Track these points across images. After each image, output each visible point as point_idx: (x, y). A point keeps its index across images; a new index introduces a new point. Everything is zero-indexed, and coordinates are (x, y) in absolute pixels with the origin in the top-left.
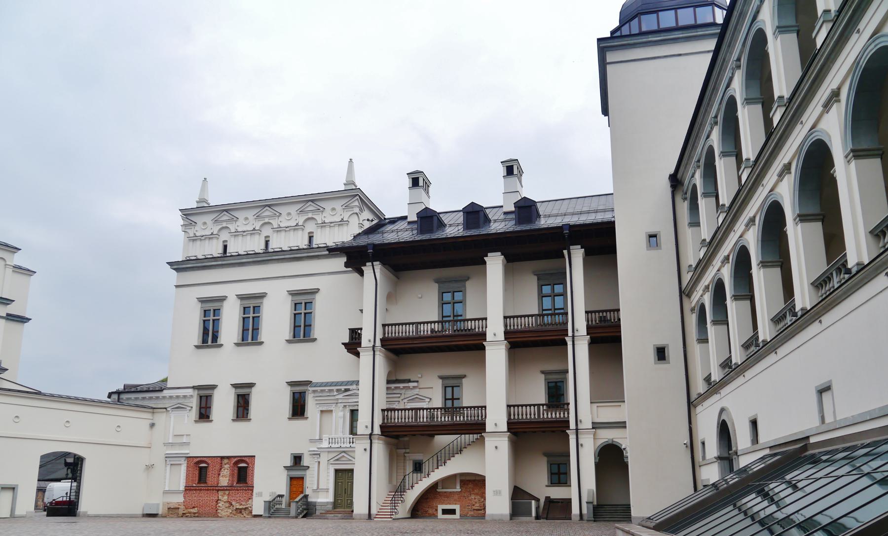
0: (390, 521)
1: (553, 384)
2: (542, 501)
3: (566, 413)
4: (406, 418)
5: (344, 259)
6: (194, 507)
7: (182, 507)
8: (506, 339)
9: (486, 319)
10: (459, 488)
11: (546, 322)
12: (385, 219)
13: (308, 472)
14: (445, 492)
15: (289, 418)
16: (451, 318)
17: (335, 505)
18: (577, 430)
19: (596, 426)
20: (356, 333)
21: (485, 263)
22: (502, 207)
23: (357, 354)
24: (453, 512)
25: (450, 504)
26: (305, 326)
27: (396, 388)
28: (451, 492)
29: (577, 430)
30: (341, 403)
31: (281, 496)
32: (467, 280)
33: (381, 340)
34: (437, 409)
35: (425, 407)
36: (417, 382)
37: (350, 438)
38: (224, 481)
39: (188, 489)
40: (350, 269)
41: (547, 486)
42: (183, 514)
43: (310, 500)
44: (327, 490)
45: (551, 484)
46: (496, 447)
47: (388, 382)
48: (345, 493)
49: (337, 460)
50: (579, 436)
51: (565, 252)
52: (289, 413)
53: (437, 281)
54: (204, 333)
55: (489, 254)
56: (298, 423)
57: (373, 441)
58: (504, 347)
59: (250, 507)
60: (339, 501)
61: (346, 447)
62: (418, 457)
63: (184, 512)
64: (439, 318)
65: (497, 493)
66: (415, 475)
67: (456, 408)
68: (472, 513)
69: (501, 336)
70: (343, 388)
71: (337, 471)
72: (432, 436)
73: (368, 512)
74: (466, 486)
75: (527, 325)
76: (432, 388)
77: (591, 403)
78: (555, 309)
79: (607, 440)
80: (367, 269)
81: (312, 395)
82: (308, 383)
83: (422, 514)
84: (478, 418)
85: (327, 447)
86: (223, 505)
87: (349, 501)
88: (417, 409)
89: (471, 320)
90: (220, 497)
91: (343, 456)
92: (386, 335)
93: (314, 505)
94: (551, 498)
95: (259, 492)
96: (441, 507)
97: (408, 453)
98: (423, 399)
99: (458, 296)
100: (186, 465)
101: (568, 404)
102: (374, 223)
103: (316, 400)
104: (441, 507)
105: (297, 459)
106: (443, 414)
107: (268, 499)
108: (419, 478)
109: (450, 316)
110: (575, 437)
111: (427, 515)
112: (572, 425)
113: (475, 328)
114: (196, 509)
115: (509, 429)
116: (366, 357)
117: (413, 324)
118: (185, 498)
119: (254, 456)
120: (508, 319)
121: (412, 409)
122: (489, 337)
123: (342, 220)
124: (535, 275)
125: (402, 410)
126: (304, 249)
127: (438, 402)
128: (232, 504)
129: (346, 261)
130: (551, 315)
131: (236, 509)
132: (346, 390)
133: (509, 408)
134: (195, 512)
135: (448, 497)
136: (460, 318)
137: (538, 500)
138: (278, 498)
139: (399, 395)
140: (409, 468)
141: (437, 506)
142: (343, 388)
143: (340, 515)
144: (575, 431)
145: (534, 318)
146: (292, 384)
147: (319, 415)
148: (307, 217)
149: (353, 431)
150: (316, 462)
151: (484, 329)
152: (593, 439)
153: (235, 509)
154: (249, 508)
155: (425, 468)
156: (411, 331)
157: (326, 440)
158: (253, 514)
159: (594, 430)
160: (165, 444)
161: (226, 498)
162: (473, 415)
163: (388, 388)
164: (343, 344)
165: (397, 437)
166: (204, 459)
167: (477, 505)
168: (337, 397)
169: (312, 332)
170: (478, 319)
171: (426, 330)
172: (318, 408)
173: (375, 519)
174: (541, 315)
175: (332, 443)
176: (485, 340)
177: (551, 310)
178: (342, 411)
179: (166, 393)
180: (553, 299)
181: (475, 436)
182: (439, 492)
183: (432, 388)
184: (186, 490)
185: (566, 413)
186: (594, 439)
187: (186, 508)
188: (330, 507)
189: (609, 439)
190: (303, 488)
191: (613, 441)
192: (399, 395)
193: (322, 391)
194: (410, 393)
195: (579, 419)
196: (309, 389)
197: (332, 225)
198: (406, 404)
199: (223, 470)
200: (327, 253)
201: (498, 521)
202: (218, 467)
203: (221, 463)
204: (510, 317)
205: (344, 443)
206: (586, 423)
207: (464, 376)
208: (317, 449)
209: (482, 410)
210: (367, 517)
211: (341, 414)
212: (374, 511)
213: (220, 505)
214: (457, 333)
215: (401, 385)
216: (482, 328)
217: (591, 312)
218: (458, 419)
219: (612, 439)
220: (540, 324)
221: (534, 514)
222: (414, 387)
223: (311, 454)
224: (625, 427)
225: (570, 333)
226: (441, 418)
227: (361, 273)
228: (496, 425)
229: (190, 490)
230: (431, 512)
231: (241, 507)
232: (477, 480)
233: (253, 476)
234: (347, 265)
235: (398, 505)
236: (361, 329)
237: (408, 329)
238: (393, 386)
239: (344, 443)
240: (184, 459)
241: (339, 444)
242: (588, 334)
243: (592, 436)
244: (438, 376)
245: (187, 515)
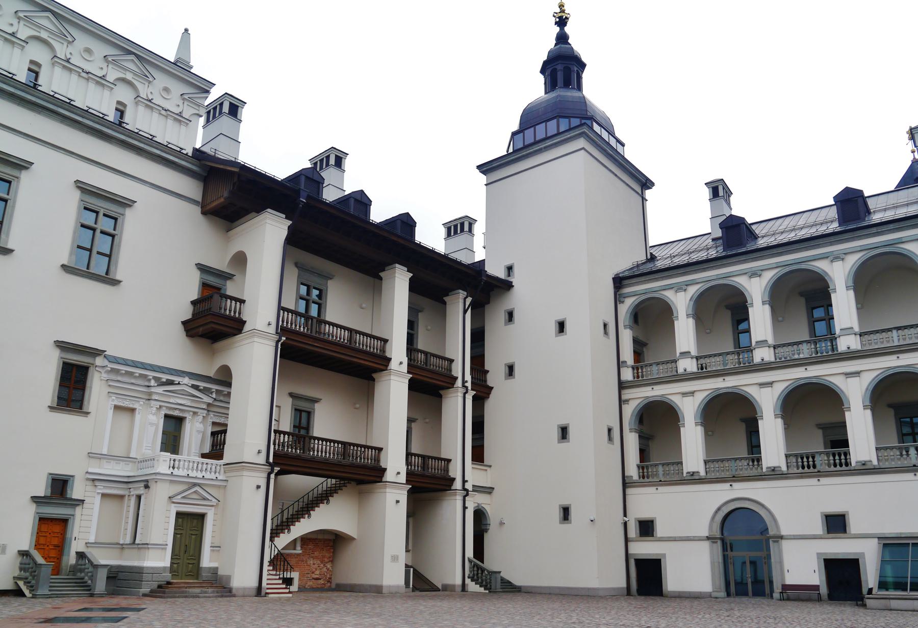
0: (288, 599)
10: (299, 548)
15: (50, 407)
44: (163, 547)
49: (205, 499)
61: (196, 478)
68: (311, 583)
74: (305, 546)
82: (95, 353)
103: (109, 385)
132: (170, 383)
142: (165, 377)
146: (62, 346)
148: (123, 76)
150: (98, 493)
157: (166, 461)
160: (91, 455)
167: (317, 572)
168: (153, 390)
193: (128, 374)
210: (254, 592)
221: (411, 586)
223: (88, 479)
232: (320, 539)
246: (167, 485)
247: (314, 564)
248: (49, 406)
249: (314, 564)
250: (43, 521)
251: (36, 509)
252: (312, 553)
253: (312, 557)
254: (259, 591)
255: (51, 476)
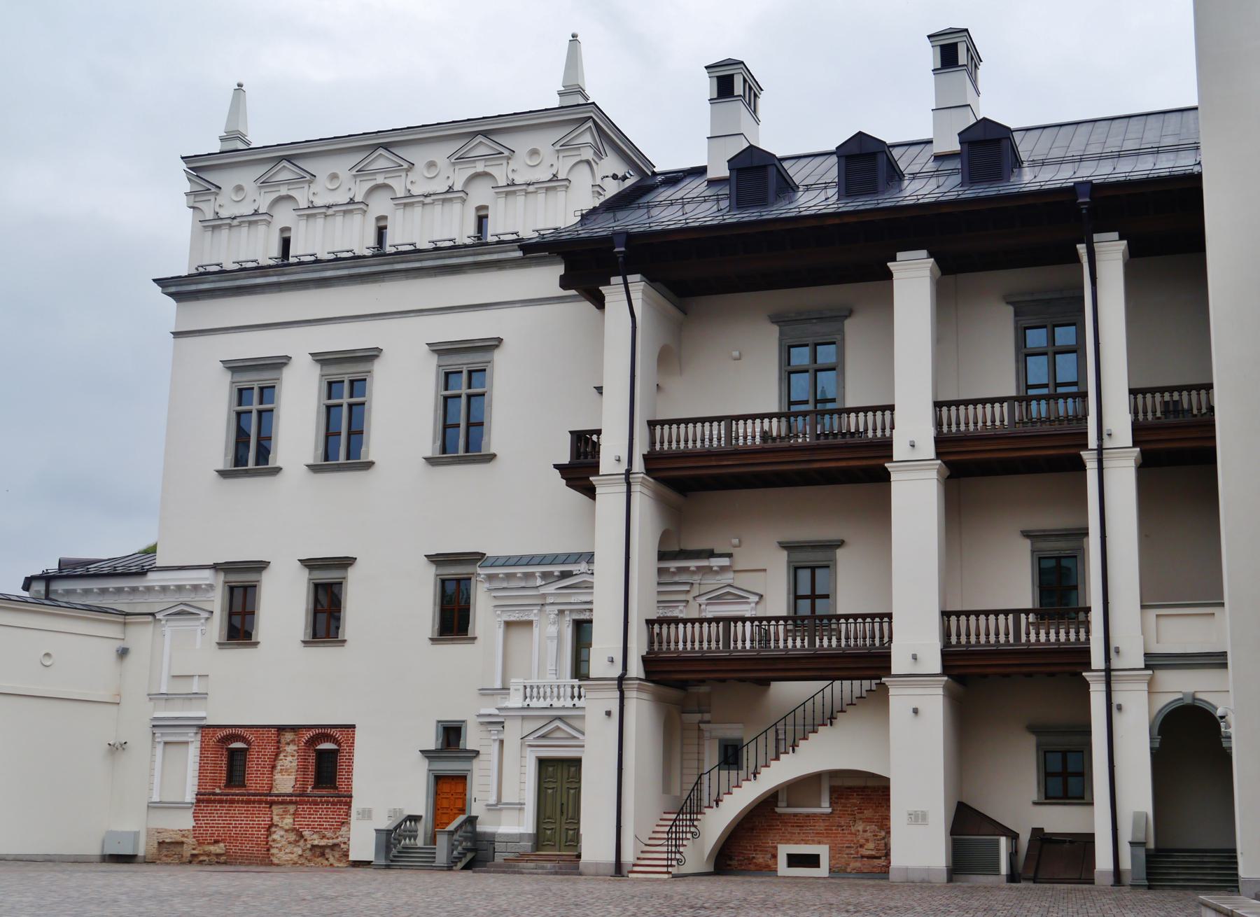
0: (665, 880)
1: (1052, 563)
2: (1025, 838)
3: (1082, 631)
4: (705, 641)
5: (560, 270)
6: (216, 842)
7: (191, 840)
8: (939, 455)
9: (891, 408)
10: (828, 805)
11: (1034, 415)
12: (654, 174)
13: (476, 765)
14: (795, 815)
15: (432, 639)
16: (810, 407)
17: (539, 840)
18: (1108, 671)
19: (1155, 662)
20: (587, 440)
21: (889, 276)
22: (930, 142)
23: (590, 492)
24: (813, 861)
25: (806, 842)
26: (469, 425)
27: (681, 570)
28: (808, 815)
29: (1108, 671)
30: (552, 604)
31: (415, 819)
32: (846, 317)
33: (646, 458)
34: (777, 619)
35: (748, 615)
36: (730, 555)
37: (573, 687)
38: (285, 783)
39: (203, 799)
40: (573, 292)
41: (1035, 803)
42: (193, 856)
43: (481, 828)
44: (520, 806)
45: (1046, 798)
46: (916, 711)
47: (662, 556)
48: (562, 812)
49: (543, 737)
50: (1114, 686)
51: (1082, 248)
52: (433, 626)
53: (777, 319)
54: (237, 443)
55: (900, 255)
56: (454, 651)
57: (627, 694)
58: (934, 474)
59: (345, 843)
60: (549, 832)
61: (564, 708)
62: (732, 731)
63: (194, 852)
64: (780, 407)
65: (918, 818)
66: (724, 773)
67: (821, 618)
68: (858, 864)
69: (927, 448)
70: (557, 569)
71: (542, 763)
72: (766, 683)
73: (614, 859)
74: (843, 801)
75: (989, 423)
76: (765, 570)
77: (1143, 607)
78: (1057, 385)
79: (1180, 696)
80: (613, 293)
81: (487, 585)
82: (476, 558)
83: (741, 865)
84: (873, 641)
85: (520, 705)
86: (282, 837)
87: (571, 832)
88: (728, 621)
89: (857, 410)
90: (276, 818)
91: (558, 728)
92: (658, 447)
93: (490, 839)
94: (1046, 831)
95: (364, 810)
96: (784, 850)
97: (709, 722)
98: (743, 597)
99: (826, 354)
100: (198, 744)
101: (1088, 610)
102: (629, 183)
103: (494, 597)
104: (784, 850)
105: (451, 734)
106: (790, 631)
107: (386, 824)
108: (733, 782)
109: (806, 402)
110: (1103, 687)
111: (752, 866)
112: (1097, 660)
113: (866, 430)
114: (222, 845)
115: (947, 669)
116: (610, 497)
117: (719, 419)
118: (196, 819)
119: (353, 726)
120: (945, 409)
121: (717, 620)
122: (899, 451)
123: (555, 178)
124: (1008, 303)
125: (693, 621)
126: (466, 246)
127: (778, 604)
128: (302, 836)
129: (562, 272)
130: (1047, 398)
131: (313, 846)
132: (565, 575)
133: (946, 619)
134: (219, 851)
135: (801, 826)
136: (829, 406)
137: (1013, 836)
138: (408, 823)
139: (687, 588)
140: (711, 756)
141: (776, 848)
142: (557, 569)
143: (549, 865)
144: (1103, 673)
145: (1005, 405)
146: (438, 560)
147: (500, 632)
149: (579, 669)
150: (495, 740)
151: (888, 433)
152: (1146, 692)
153: (309, 846)
154: (342, 846)
155: (749, 756)
156: (714, 436)
157: (519, 690)
158: (352, 857)
159: (1150, 672)
161: (288, 821)
162: (860, 634)
163: (661, 571)
164: (556, 466)
165: (682, 685)
166: (239, 731)
167: (871, 845)
168: (543, 591)
169: (485, 438)
170: (874, 409)
171: (749, 434)
172: (499, 616)
173: (631, 875)
174: (1022, 400)
175: (532, 698)
176: (890, 458)
177: (1046, 386)
178: (554, 623)
179: (154, 579)
180: (1051, 359)
181: (866, 684)
182: (780, 815)
183: (765, 570)
184: (198, 801)
185: (1082, 631)
186: (1149, 692)
187: (200, 844)
188: (527, 845)
189: (1184, 694)
190: (464, 800)
191: (1194, 699)
192: (687, 588)
193: (509, 576)
194: (712, 583)
195: (1113, 644)
196: (479, 571)
197: (531, 188)
198: (703, 607)
199: (281, 756)
200: (519, 254)
201: (918, 884)
202: (271, 749)
203: (279, 742)
204: (949, 404)
205: (559, 698)
206: (1131, 656)
207: (841, 544)
208: (496, 712)
209: (881, 623)
210: (612, 870)
211: (552, 630)
212: (628, 857)
213: (275, 836)
214: (822, 441)
215: (692, 564)
216: (883, 429)
217: (1144, 391)
218: (826, 643)
219: (1193, 695)
220: (1021, 420)
221: (1004, 868)
222: (723, 569)
223: (482, 723)
224: (1224, 666)
225: (1092, 442)
226: (786, 641)
227: (599, 302)
228: (915, 657)
229: (209, 801)
230: (761, 860)
231: (323, 842)
233: (350, 772)
234: (565, 283)
235: (685, 842)
236: (598, 432)
237: (707, 433)
238: (673, 565)
239: (559, 698)
240: (194, 730)
241: (548, 699)
242: (1135, 444)
243: (1145, 687)
244: (779, 543)
245: (201, 858)
246: (518, 722)
247: (865, 831)
248: (430, 639)
249: (865, 831)
250: (439, 779)
251: (429, 765)
252: (858, 813)
253: (861, 819)
254: (619, 868)
255: (440, 723)
